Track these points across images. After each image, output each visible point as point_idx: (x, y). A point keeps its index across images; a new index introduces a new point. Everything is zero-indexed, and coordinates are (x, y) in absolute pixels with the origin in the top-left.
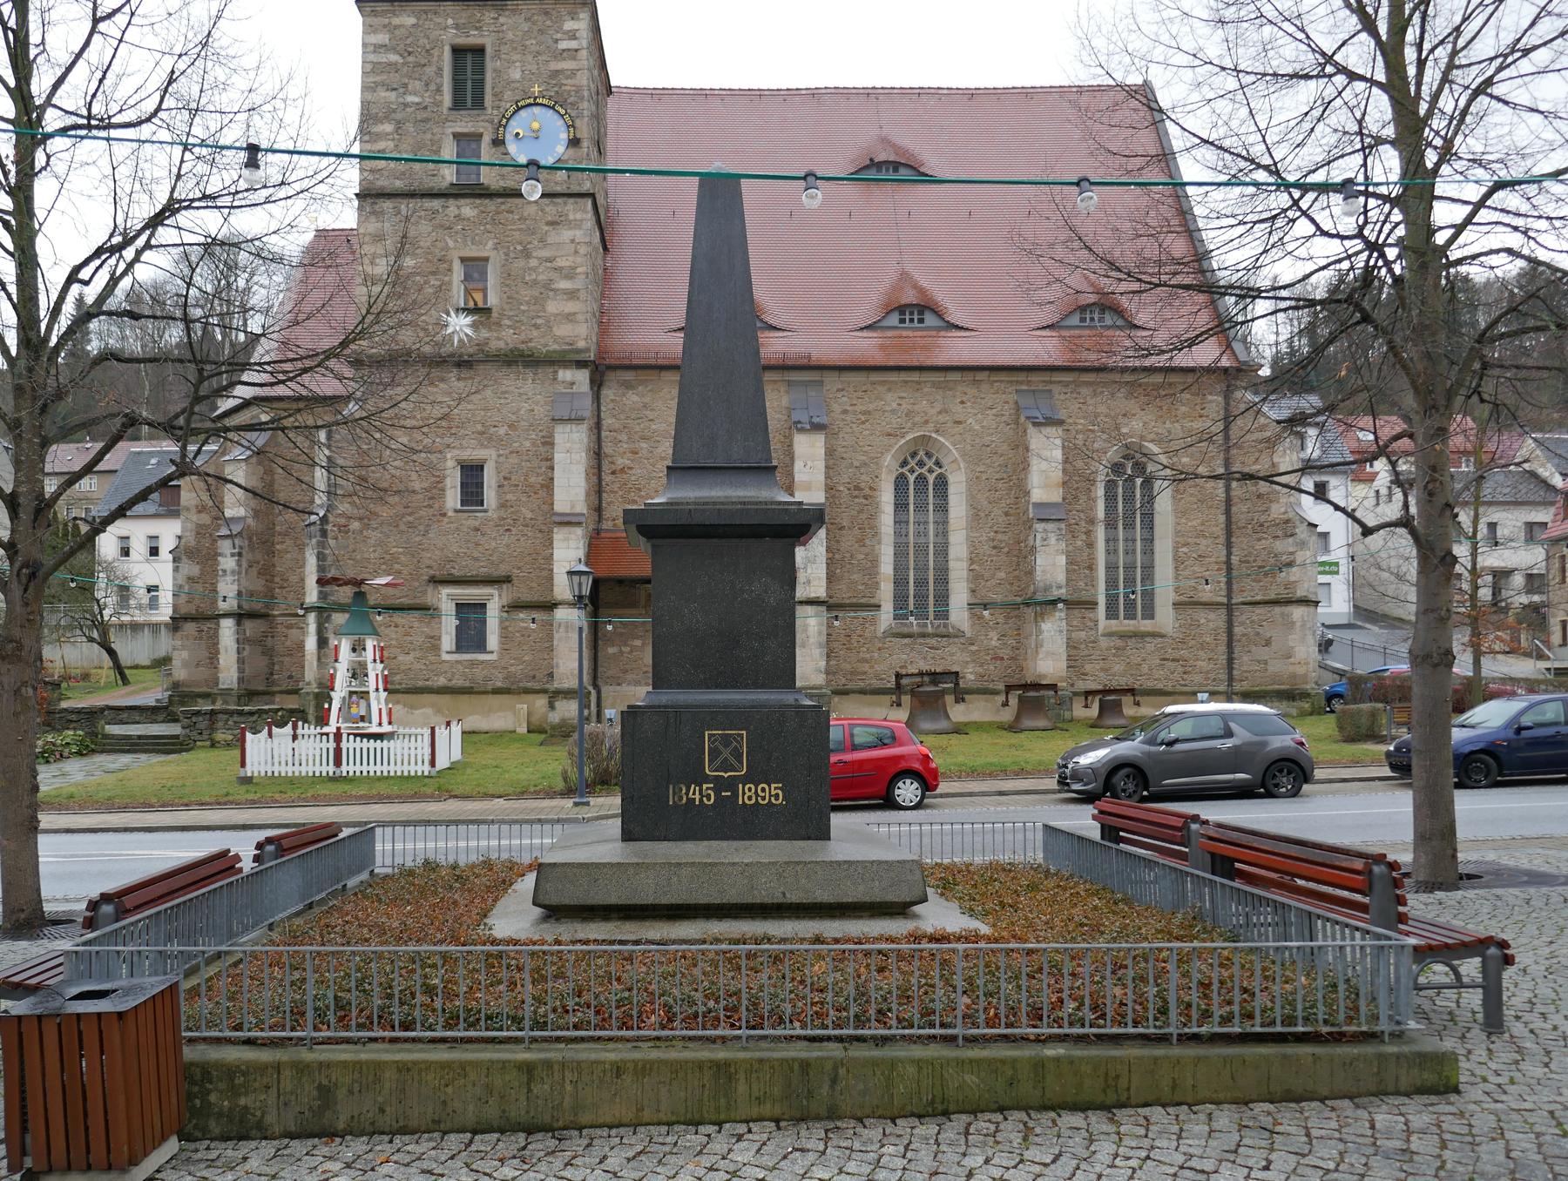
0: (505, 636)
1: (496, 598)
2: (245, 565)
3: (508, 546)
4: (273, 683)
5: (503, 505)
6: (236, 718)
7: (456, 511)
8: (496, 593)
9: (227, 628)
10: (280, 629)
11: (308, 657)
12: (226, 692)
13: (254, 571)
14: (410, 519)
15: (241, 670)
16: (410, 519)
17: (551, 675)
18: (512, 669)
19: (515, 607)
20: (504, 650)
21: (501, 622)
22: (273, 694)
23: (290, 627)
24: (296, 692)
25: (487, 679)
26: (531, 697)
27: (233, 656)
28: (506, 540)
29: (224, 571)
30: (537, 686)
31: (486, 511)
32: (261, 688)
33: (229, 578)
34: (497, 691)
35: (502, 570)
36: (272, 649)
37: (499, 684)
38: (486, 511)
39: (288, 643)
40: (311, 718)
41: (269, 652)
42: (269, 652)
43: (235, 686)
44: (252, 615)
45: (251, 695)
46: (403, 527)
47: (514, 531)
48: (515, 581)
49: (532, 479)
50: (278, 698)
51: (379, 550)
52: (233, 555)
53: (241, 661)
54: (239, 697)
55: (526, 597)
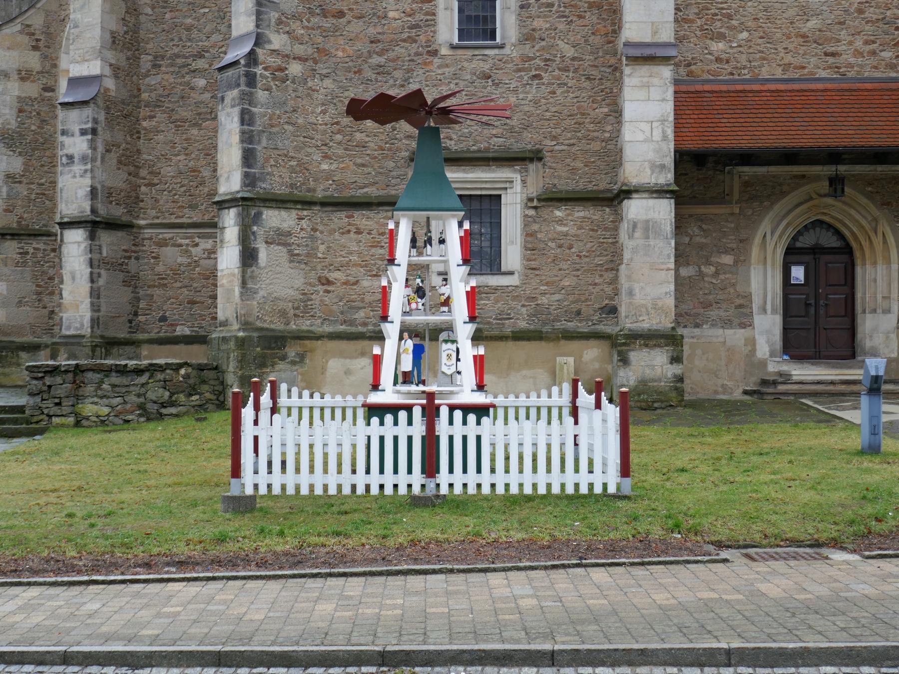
0: (532, 246)
1: (518, 186)
2: (101, 149)
3: (536, 102)
5: (528, 37)
6: (115, 379)
7: (453, 47)
8: (517, 177)
9: (75, 246)
10: (148, 246)
11: (223, 281)
12: (73, 341)
13: (113, 157)
14: (382, 60)
15: (95, 308)
16: (382, 60)
18: (544, 300)
20: (531, 269)
21: (527, 222)
23: (163, 244)
25: (503, 317)
26: (575, 345)
27: (84, 286)
28: (533, 92)
29: (70, 157)
30: (583, 327)
31: (501, 47)
32: (122, 335)
33: (77, 168)
34: (519, 336)
35: (527, 141)
36: (136, 277)
37: (523, 324)
38: (501, 47)
39: (160, 268)
41: (131, 281)
42: (131, 281)
43: (87, 331)
44: (112, 225)
45: (110, 344)
46: (368, 74)
48: (548, 159)
52: (83, 132)
53: (95, 294)
54: (94, 348)
55: (566, 184)
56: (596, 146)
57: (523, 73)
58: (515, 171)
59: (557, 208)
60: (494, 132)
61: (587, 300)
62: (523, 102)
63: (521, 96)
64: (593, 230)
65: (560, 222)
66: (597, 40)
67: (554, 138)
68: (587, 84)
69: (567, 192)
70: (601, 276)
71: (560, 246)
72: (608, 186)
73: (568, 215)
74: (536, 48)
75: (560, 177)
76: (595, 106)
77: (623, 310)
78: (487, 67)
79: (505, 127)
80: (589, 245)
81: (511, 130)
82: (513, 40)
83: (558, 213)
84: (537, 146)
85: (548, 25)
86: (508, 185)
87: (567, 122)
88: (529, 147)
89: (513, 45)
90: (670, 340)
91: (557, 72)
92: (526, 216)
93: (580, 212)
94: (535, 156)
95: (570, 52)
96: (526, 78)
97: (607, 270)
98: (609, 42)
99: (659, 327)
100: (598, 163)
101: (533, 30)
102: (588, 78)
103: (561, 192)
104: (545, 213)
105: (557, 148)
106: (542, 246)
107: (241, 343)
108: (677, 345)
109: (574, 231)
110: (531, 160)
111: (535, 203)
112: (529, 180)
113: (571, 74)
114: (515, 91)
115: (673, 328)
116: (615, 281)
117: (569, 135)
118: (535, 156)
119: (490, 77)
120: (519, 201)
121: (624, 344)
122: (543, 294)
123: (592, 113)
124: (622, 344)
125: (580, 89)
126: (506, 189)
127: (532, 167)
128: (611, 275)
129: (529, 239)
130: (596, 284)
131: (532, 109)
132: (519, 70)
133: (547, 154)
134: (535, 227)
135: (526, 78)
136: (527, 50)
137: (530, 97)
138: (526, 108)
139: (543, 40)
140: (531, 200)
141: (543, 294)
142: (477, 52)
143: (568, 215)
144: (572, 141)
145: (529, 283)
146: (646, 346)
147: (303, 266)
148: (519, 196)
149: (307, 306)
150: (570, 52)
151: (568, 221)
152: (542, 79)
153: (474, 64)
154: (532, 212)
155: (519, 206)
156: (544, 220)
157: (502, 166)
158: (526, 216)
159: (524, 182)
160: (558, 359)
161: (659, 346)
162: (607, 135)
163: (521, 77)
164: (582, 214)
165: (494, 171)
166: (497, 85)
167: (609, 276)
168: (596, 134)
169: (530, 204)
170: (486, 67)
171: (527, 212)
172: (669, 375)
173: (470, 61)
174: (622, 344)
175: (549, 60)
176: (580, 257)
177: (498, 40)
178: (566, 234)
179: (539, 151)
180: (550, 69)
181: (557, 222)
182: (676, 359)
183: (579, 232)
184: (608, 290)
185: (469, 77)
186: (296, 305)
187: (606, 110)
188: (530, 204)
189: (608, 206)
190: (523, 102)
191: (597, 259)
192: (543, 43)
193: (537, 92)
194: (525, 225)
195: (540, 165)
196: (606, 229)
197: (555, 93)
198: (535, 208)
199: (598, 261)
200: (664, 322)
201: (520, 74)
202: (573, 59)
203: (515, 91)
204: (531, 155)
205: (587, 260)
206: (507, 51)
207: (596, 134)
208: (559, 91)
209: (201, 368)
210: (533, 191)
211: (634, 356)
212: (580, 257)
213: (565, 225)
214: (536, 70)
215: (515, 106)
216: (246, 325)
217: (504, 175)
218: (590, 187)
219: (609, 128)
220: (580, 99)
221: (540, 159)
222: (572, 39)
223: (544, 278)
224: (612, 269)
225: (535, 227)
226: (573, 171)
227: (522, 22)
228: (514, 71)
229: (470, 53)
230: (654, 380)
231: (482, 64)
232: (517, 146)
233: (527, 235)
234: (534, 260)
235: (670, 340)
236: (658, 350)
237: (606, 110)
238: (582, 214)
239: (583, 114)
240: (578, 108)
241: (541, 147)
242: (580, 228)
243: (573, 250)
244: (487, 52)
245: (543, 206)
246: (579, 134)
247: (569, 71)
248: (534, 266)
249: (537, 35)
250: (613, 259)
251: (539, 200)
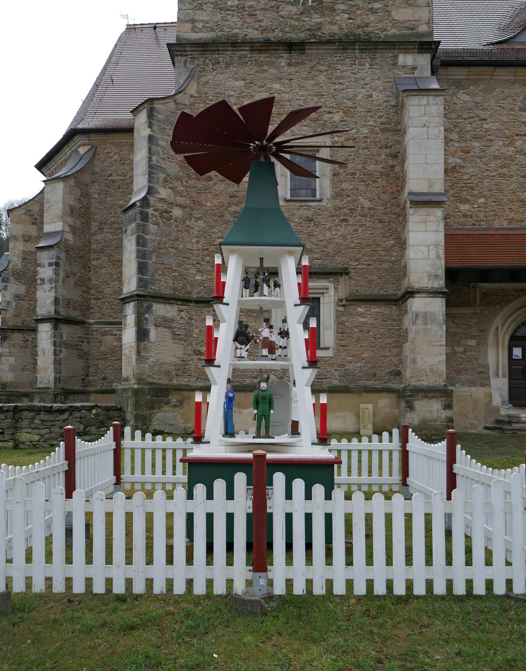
1: (332, 292)
3: (344, 237)
4: (89, 384)
5: (338, 195)
8: (331, 286)
17: (398, 374)
19: (355, 300)
20: (340, 346)
21: (338, 315)
22: (88, 393)
24: (112, 392)
28: (342, 230)
31: (320, 201)
35: (338, 262)
38: (320, 201)
40: (130, 417)
47: (351, 220)
48: (352, 273)
49: (371, 167)
50: (93, 397)
51: (203, 241)
55: (365, 291)
56: (386, 266)
57: (335, 218)
58: (330, 282)
59: (360, 306)
60: (315, 256)
61: (380, 367)
62: (335, 237)
63: (334, 233)
64: (384, 321)
65: (361, 315)
66: (386, 197)
67: (357, 260)
68: (379, 225)
69: (366, 295)
70: (390, 351)
71: (361, 331)
72: (395, 292)
73: (367, 311)
74: (344, 202)
75: (361, 286)
76: (385, 239)
77: (408, 373)
78: (311, 213)
79: (323, 253)
80: (382, 330)
81: (328, 254)
82: (328, 196)
83: (360, 309)
84: (345, 266)
85: (352, 187)
86: (325, 291)
87: (366, 250)
88: (340, 266)
89: (328, 199)
90: (444, 394)
91: (358, 217)
92: (337, 311)
93: (375, 309)
94: (345, 272)
95: (367, 204)
96: (337, 221)
97: (394, 347)
98: (395, 198)
99: (435, 384)
100: (388, 277)
101: (342, 190)
102: (380, 222)
103: (362, 295)
104: (351, 309)
105: (359, 267)
106: (349, 331)
107: (136, 392)
108: (448, 397)
109: (371, 321)
110: (341, 274)
111: (344, 302)
112: (340, 287)
113: (368, 219)
114: (330, 229)
115: (445, 385)
116: (399, 354)
117: (367, 258)
118: (345, 272)
119: (312, 220)
120: (332, 301)
121: (410, 396)
122: (350, 362)
123: (383, 244)
124: (408, 396)
125: (374, 228)
126: (323, 293)
127: (342, 279)
128: (396, 350)
129: (340, 326)
130: (386, 356)
131: (341, 241)
132: (332, 216)
133: (352, 271)
134: (344, 318)
135: (337, 221)
136: (338, 203)
137: (340, 233)
138: (337, 241)
139: (349, 196)
140: (341, 300)
141: (350, 362)
142: (303, 204)
143: (367, 311)
144: (369, 263)
145: (340, 355)
146: (426, 397)
147: (182, 342)
148: (332, 297)
149: (185, 369)
150: (367, 204)
151: (366, 314)
152: (348, 221)
153: (301, 212)
154: (341, 309)
155: (332, 305)
156: (350, 314)
157: (321, 278)
158: (337, 311)
159: (336, 289)
160: (361, 405)
161: (436, 397)
162: (394, 258)
163: (334, 220)
164: (376, 310)
165: (315, 282)
166: (317, 225)
167: (395, 351)
168: (386, 258)
169: (340, 303)
170: (310, 214)
171: (338, 309)
172: (443, 417)
173: (298, 209)
174: (408, 396)
175: (353, 209)
176: (375, 338)
177: (318, 197)
178: (365, 323)
179: (347, 269)
180: (354, 215)
181: (359, 315)
182: (448, 407)
183: (375, 322)
184: (395, 360)
185: (297, 220)
186: (177, 368)
187: (393, 242)
188: (340, 303)
189: (394, 305)
190: (335, 237)
191: (387, 340)
192: (349, 199)
193: (345, 230)
194: (337, 317)
195: (347, 278)
196: (393, 320)
197: (357, 231)
198: (344, 306)
199: (387, 341)
200: (439, 381)
201: (332, 218)
202: (370, 209)
203: (330, 229)
204: (341, 271)
205: (380, 340)
206: (324, 203)
207: (386, 258)
208: (360, 230)
209: (108, 409)
210: (342, 294)
211: (417, 404)
212: (375, 338)
213: (365, 317)
214: (344, 216)
215: (330, 239)
216: (140, 380)
217: (322, 284)
218: (382, 292)
219: (395, 254)
220: (374, 235)
221: (347, 274)
222: (369, 196)
223: (350, 352)
224: (398, 347)
225: (344, 318)
226: (370, 282)
227: (334, 184)
228: (329, 217)
229: (298, 204)
230: (432, 421)
231: (306, 212)
232: (331, 265)
233: (338, 324)
234: (343, 340)
235: (444, 394)
236: (434, 400)
237: (393, 242)
238: (376, 310)
239: (377, 245)
240: (373, 241)
241: (348, 266)
242: (375, 319)
243: (370, 334)
244: (310, 204)
245: (350, 305)
246: (374, 258)
247: (367, 216)
248: (343, 344)
249: (344, 193)
250: (400, 338)
251: (347, 300)
